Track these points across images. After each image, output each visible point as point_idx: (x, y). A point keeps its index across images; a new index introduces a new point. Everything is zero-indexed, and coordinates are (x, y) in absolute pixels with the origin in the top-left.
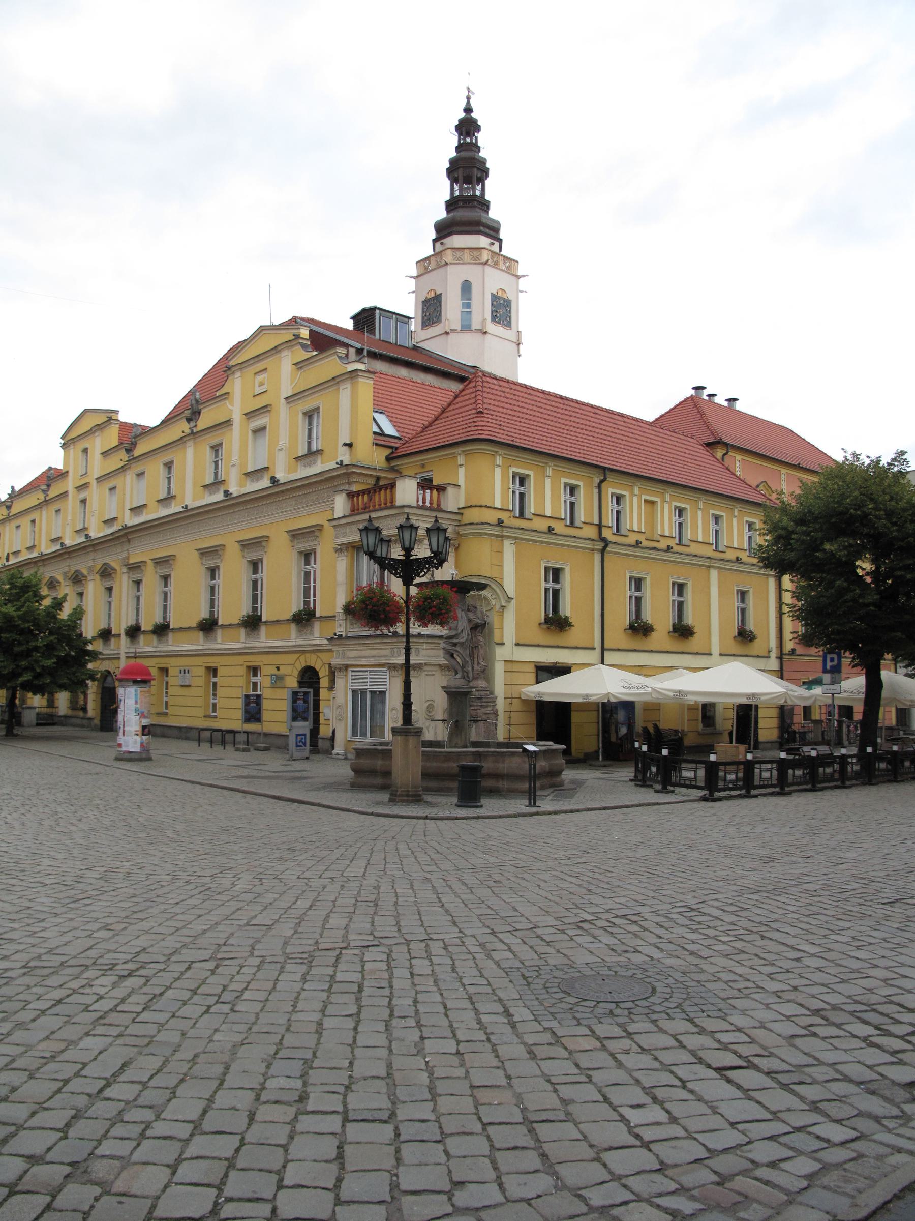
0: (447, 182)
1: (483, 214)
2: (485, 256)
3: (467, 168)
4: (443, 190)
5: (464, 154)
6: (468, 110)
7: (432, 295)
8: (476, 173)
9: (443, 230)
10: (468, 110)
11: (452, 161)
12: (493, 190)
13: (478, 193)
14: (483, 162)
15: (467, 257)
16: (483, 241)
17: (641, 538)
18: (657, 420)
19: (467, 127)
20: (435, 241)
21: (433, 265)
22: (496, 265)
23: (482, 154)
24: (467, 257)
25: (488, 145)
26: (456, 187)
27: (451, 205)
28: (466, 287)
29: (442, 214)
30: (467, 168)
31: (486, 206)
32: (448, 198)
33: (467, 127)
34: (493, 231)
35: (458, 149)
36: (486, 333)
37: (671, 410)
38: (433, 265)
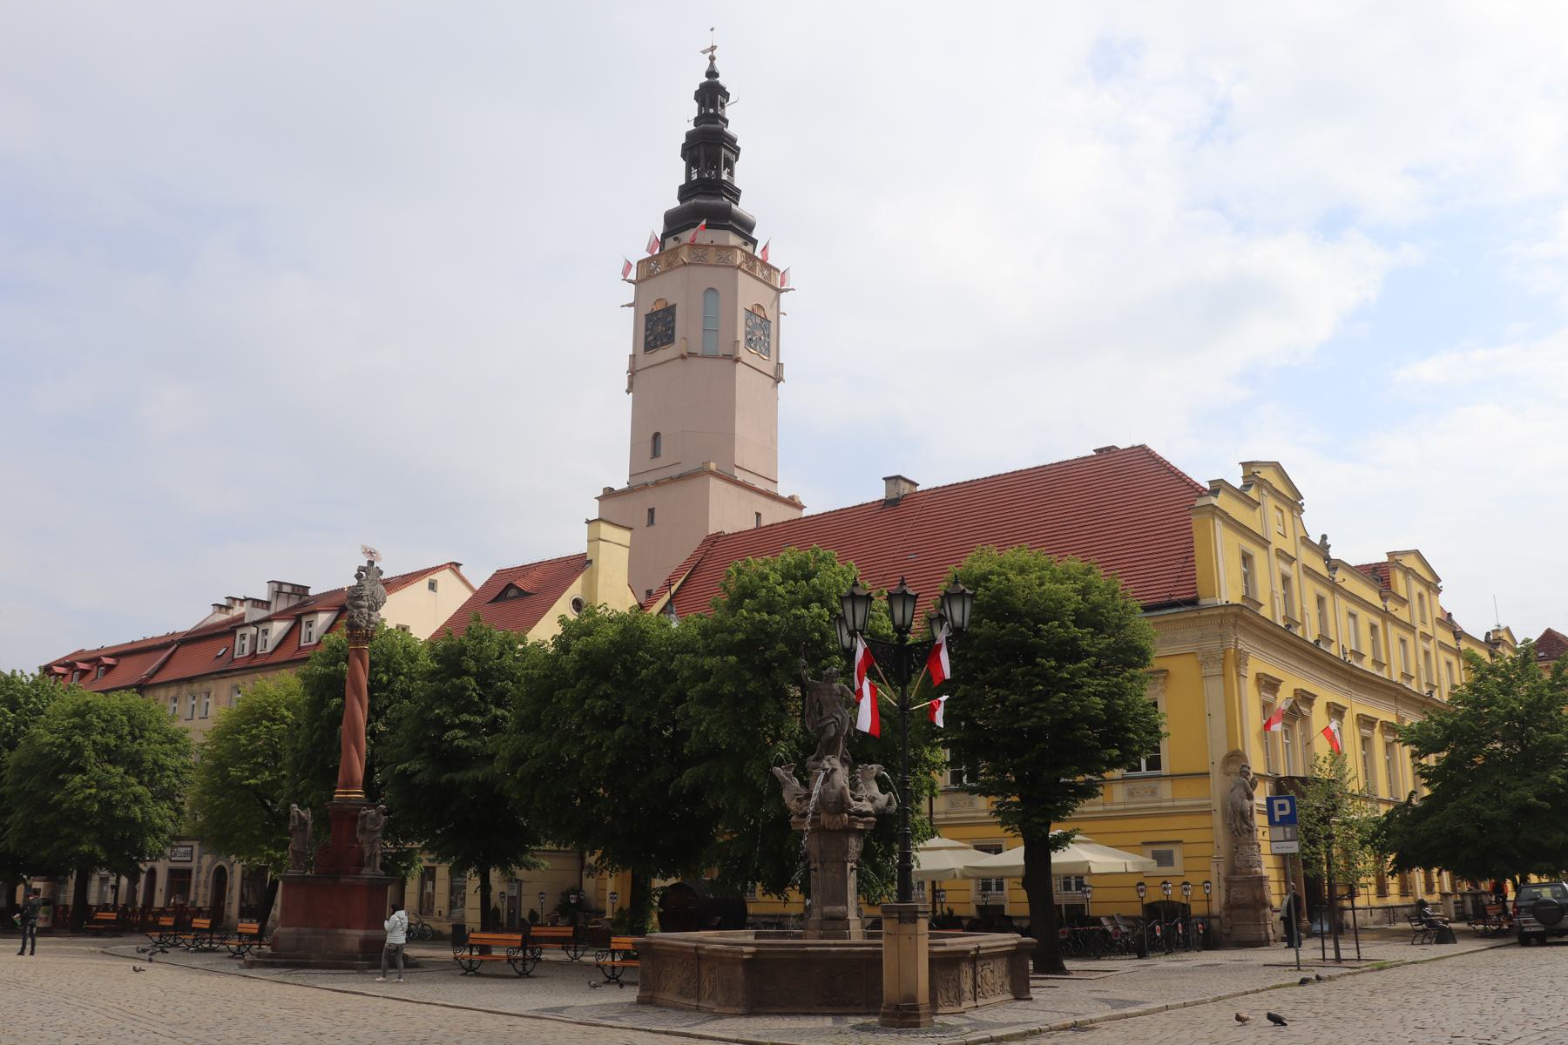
0: (683, 164)
2: (739, 258)
3: (709, 147)
4: (676, 172)
6: (712, 73)
7: (660, 306)
9: (676, 223)
10: (712, 73)
11: (689, 135)
12: (743, 175)
16: (734, 240)
19: (711, 95)
22: (750, 273)
25: (737, 121)
27: (685, 192)
30: (709, 147)
32: (683, 182)
33: (711, 95)
34: (744, 228)
35: (697, 121)
36: (737, 360)
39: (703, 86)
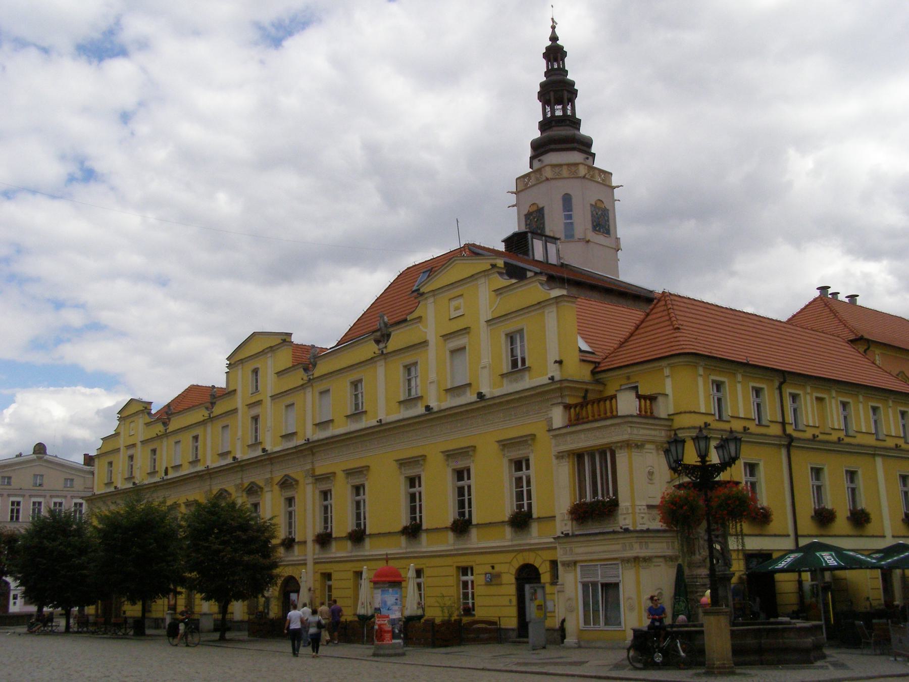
1: (576, 132)
3: (557, 90)
5: (554, 78)
8: (566, 95)
11: (543, 85)
13: (569, 113)
14: (572, 84)
15: (565, 172)
17: (817, 432)
18: (790, 320)
20: (532, 159)
21: (533, 181)
23: (570, 77)
24: (565, 172)
26: (548, 109)
28: (567, 201)
29: (537, 134)
30: (557, 90)
31: (576, 123)
35: (546, 74)
37: (802, 310)
38: (533, 181)
39: (548, 49)
